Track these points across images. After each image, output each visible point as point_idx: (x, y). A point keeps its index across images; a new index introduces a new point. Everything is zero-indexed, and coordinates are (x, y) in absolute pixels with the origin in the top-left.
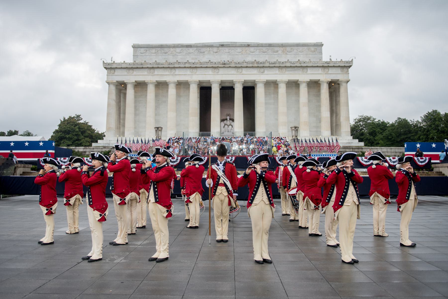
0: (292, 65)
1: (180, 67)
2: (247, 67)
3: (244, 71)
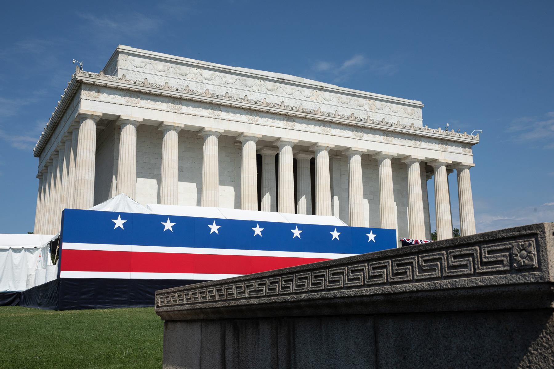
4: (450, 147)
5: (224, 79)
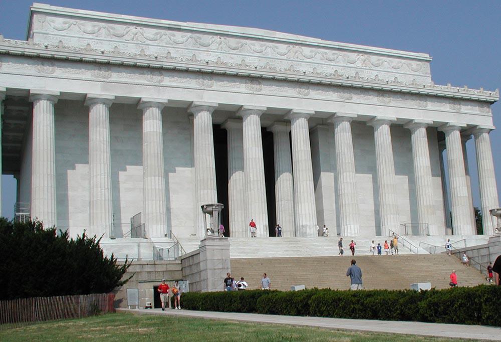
0: (405, 89)
1: (174, 71)
2: (319, 85)
3: (313, 93)
4: (463, 107)
5: (172, 38)
